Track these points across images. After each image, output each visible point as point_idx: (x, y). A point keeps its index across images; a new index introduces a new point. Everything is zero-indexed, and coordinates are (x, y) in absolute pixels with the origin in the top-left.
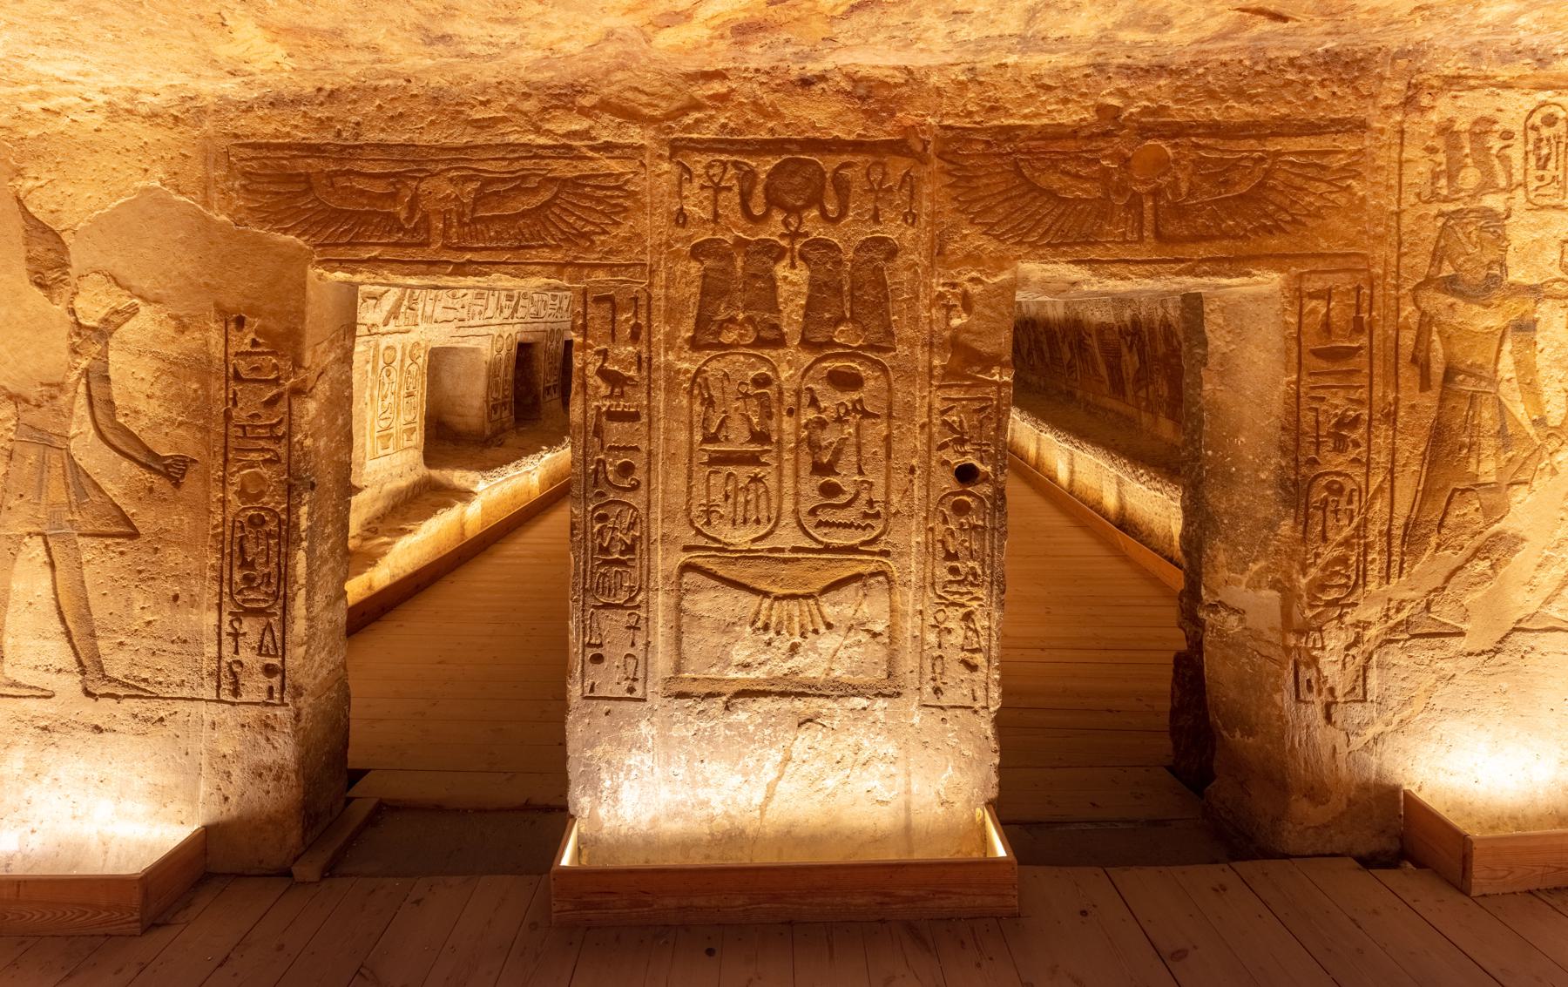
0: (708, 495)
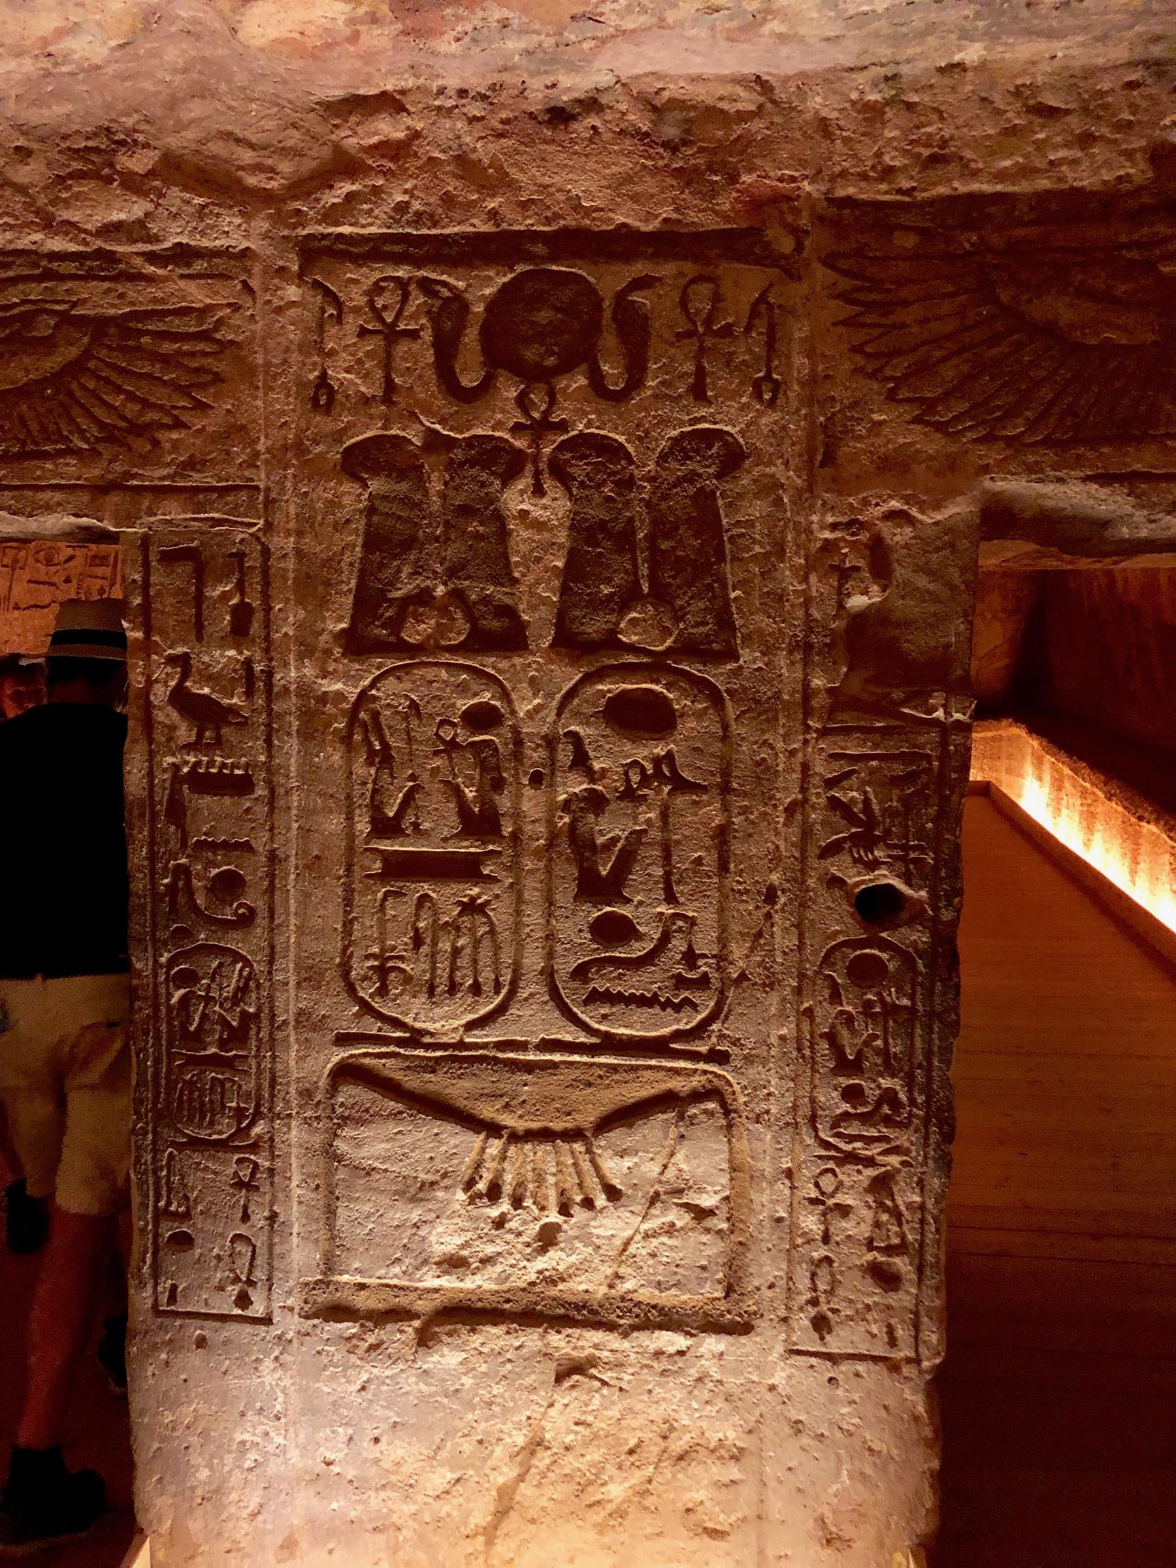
0: (382, 941)
